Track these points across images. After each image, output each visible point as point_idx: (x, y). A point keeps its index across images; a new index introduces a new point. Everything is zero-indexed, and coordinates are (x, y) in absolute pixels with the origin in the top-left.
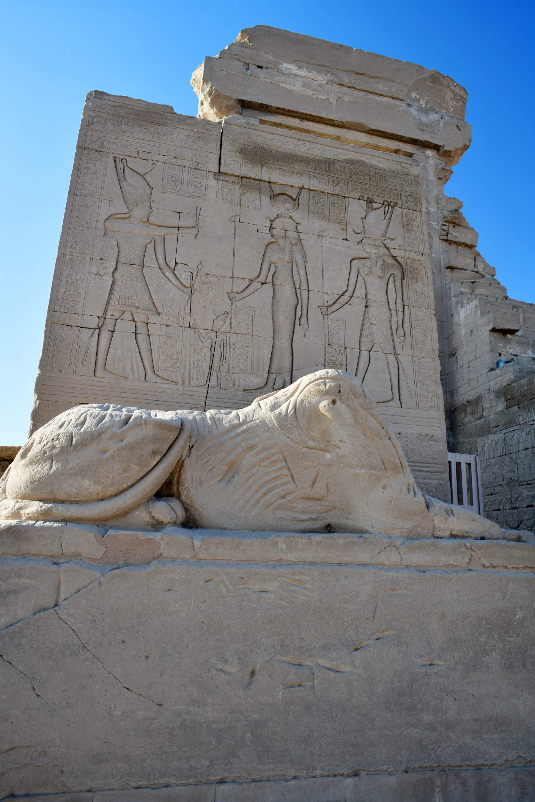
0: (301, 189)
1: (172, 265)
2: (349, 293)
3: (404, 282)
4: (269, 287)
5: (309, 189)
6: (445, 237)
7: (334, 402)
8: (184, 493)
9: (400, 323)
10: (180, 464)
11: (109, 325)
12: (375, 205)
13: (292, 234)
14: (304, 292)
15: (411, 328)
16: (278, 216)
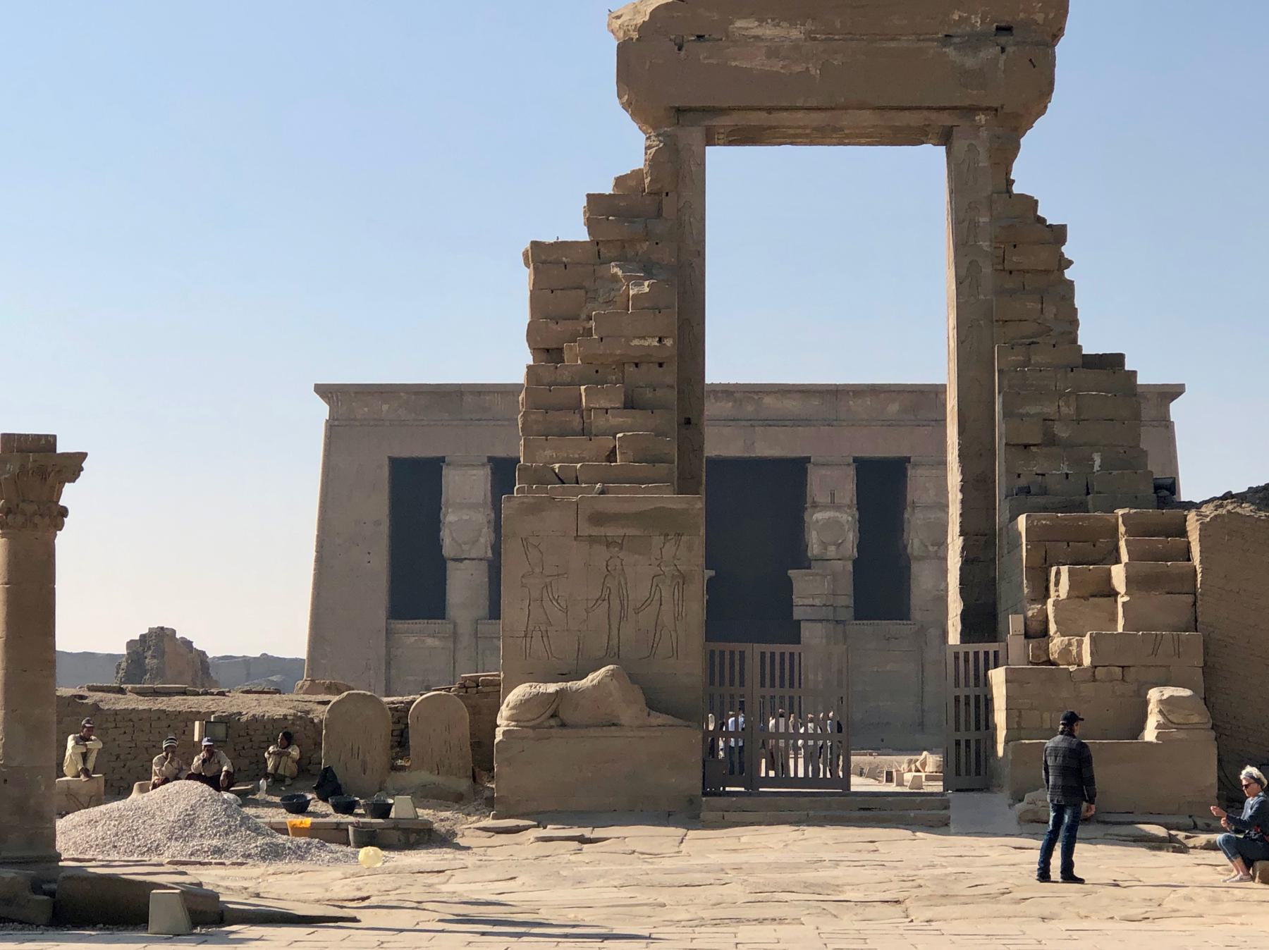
0: (625, 536)
1: (556, 597)
2: (651, 599)
3: (684, 586)
4: (607, 601)
5: (629, 536)
6: (1000, 267)
7: (612, 680)
8: (560, 715)
9: (680, 612)
10: (558, 705)
11: (529, 635)
12: (669, 537)
13: (619, 567)
14: (625, 602)
15: (686, 615)
16: (611, 557)
